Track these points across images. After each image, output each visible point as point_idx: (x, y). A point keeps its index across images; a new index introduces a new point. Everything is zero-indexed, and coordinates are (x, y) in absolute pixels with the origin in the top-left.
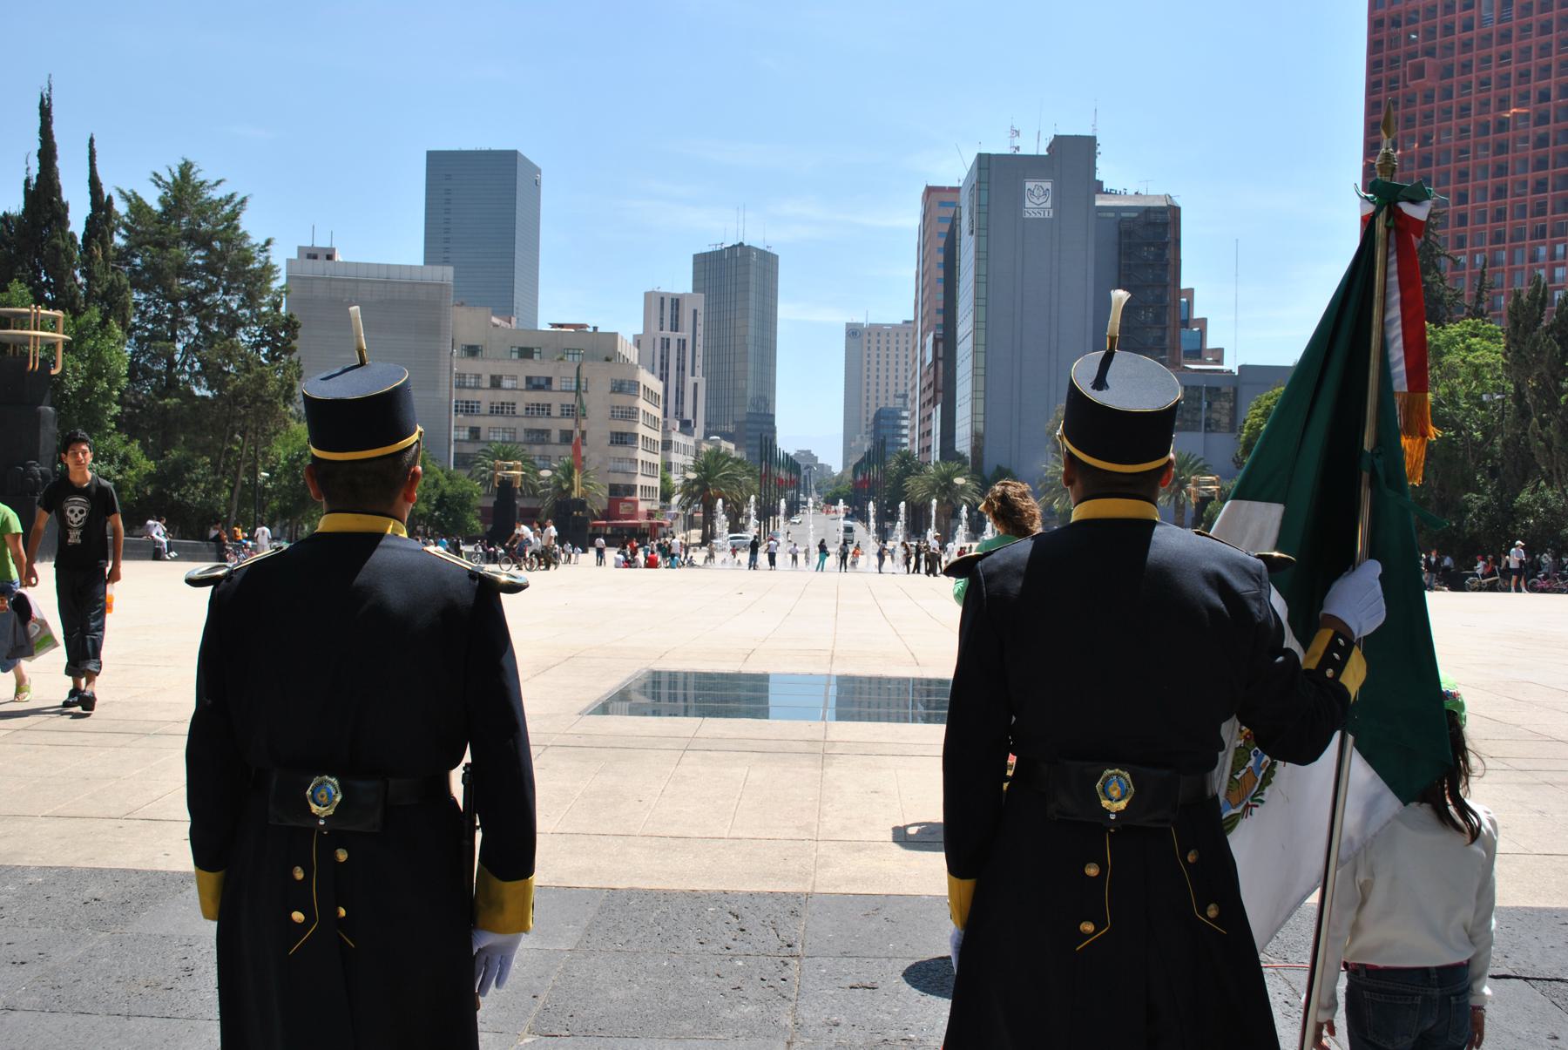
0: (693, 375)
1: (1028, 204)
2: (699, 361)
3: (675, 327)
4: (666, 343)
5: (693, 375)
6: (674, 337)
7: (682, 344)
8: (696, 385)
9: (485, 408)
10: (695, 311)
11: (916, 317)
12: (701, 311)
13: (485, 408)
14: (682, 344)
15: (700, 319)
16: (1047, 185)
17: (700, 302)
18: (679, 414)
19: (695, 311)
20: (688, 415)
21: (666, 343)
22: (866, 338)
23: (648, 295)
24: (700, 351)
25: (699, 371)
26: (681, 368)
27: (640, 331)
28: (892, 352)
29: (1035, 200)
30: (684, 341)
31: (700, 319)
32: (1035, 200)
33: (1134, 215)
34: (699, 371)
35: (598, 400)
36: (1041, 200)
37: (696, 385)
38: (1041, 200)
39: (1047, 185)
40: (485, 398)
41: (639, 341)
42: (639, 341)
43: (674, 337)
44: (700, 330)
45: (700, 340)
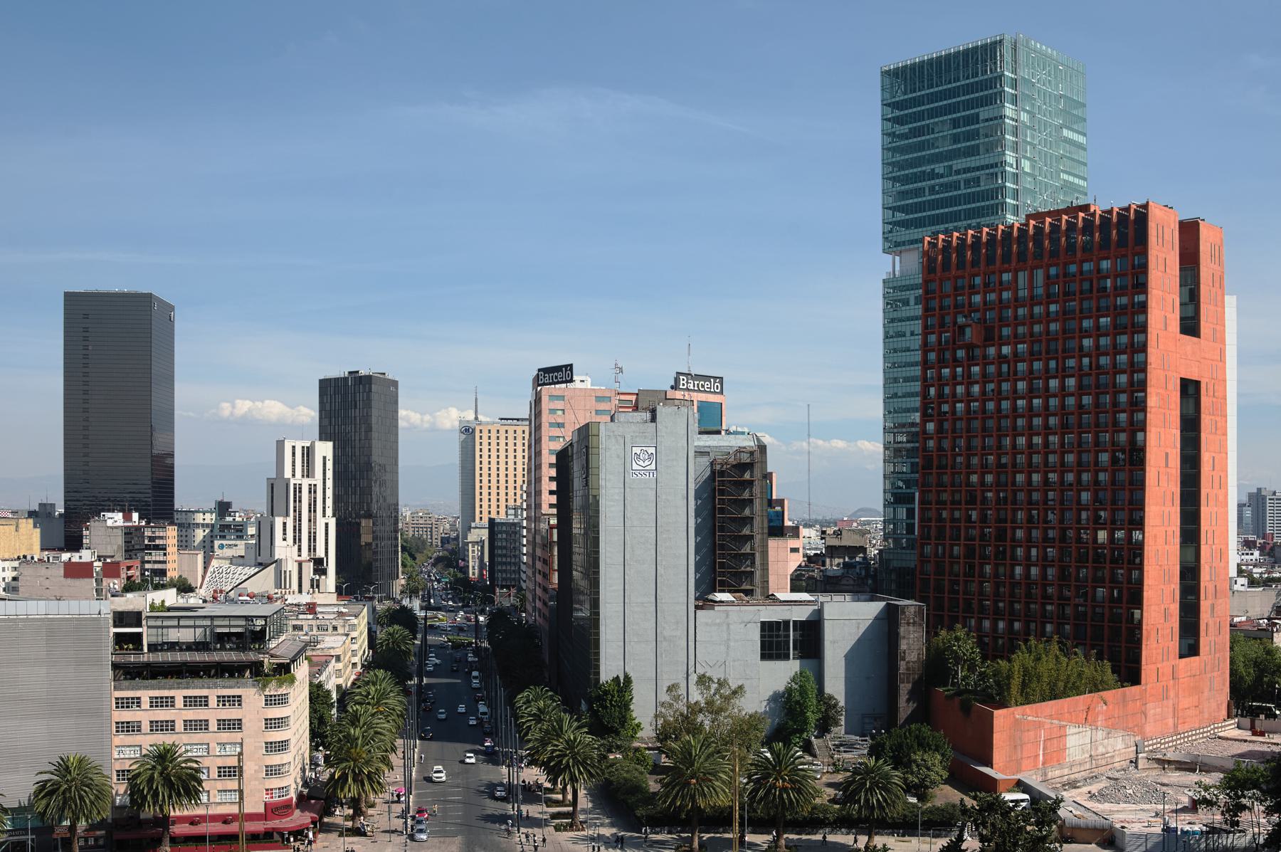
0: (324, 516)
2: (329, 502)
3: (308, 472)
5: (324, 516)
6: (306, 483)
7: (313, 490)
8: (327, 524)
10: (324, 458)
11: (530, 415)
12: (330, 456)
14: (313, 490)
15: (330, 465)
17: (325, 450)
18: (312, 548)
19: (324, 458)
20: (320, 553)
21: (298, 489)
22: (477, 434)
24: (329, 493)
25: (329, 512)
26: (312, 508)
28: (502, 447)
29: (641, 463)
30: (315, 485)
32: (641, 463)
36: (647, 463)
37: (327, 524)
38: (647, 463)
39: (652, 450)
41: (272, 484)
42: (272, 484)
43: (306, 483)
44: (330, 474)
45: (330, 483)
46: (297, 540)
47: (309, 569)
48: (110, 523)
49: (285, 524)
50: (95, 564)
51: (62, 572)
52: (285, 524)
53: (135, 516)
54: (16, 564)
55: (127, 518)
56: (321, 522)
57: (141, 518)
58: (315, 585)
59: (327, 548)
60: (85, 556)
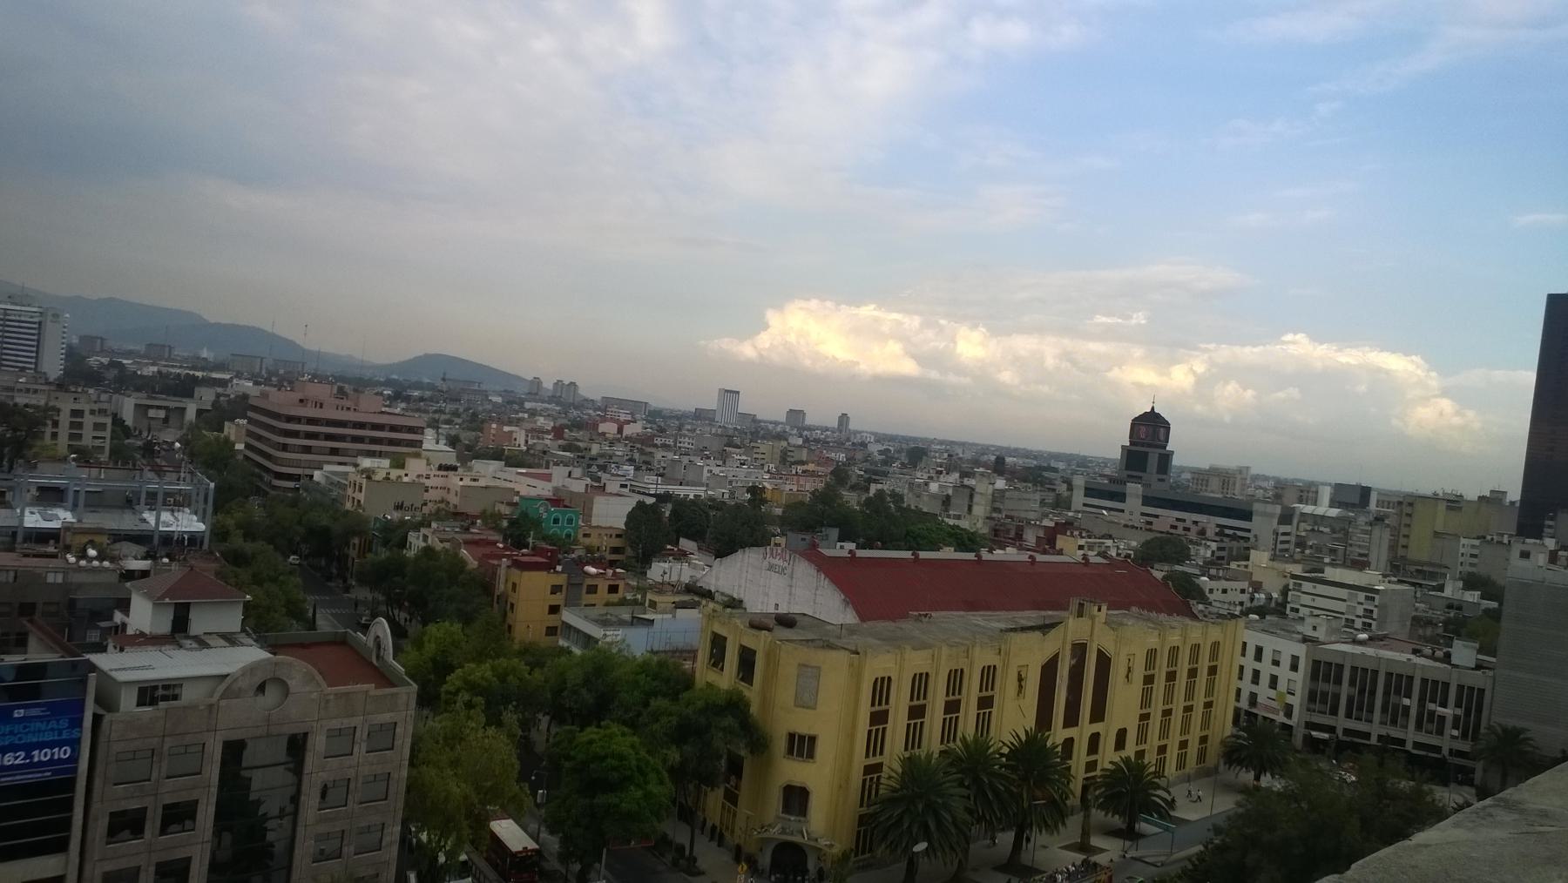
50: (1560, 553)
54: (1477, 542)
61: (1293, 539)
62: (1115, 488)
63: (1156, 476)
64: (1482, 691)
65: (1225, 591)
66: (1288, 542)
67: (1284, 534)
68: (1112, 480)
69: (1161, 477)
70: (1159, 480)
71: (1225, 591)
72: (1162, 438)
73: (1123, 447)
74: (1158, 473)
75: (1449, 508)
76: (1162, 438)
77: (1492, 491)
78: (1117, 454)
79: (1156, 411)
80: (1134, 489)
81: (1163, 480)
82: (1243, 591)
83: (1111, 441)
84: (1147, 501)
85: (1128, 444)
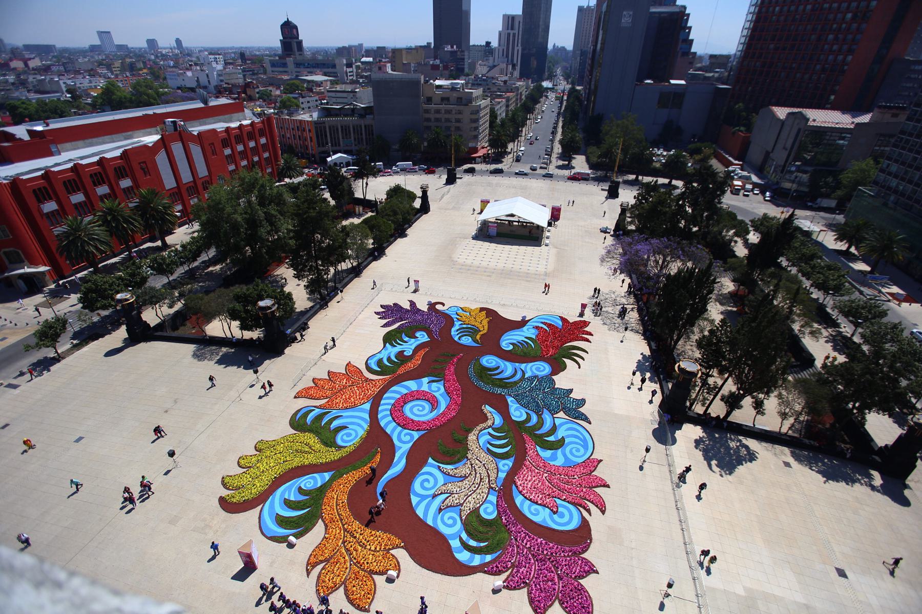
1: (623, 21)
2: (520, 41)
4: (509, 34)
5: (517, 46)
7: (514, 35)
9: (433, 120)
12: (521, 21)
13: (433, 120)
14: (514, 35)
15: (521, 24)
16: (631, 13)
20: (515, 62)
23: (504, 16)
24: (520, 37)
25: (519, 45)
27: (501, 29)
31: (521, 24)
32: (626, 19)
33: (666, 15)
34: (519, 45)
35: (466, 116)
40: (432, 116)
43: (512, 32)
44: (521, 29)
46: (507, 56)
47: (510, 67)
48: (446, 49)
49: (503, 50)
51: (430, 68)
52: (503, 50)
53: (455, 47)
55: (452, 47)
56: (516, 49)
57: (457, 47)
58: (512, 74)
59: (518, 60)
60: (438, 62)
61: (355, 74)
62: (283, 61)
63: (297, 53)
64: (372, 126)
65: (308, 102)
66: (353, 75)
67: (350, 72)
68: (280, 57)
69: (300, 53)
70: (300, 55)
71: (308, 102)
72: (295, 33)
73: (280, 40)
74: (298, 51)
75: (407, 52)
76: (295, 33)
77: (427, 43)
78: (279, 45)
79: (290, 20)
80: (290, 60)
81: (301, 54)
82: (316, 101)
83: (273, 40)
84: (298, 65)
85: (282, 38)
